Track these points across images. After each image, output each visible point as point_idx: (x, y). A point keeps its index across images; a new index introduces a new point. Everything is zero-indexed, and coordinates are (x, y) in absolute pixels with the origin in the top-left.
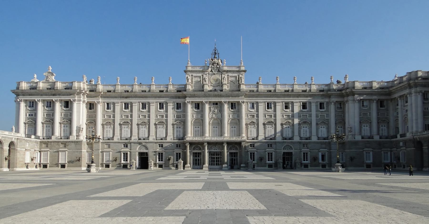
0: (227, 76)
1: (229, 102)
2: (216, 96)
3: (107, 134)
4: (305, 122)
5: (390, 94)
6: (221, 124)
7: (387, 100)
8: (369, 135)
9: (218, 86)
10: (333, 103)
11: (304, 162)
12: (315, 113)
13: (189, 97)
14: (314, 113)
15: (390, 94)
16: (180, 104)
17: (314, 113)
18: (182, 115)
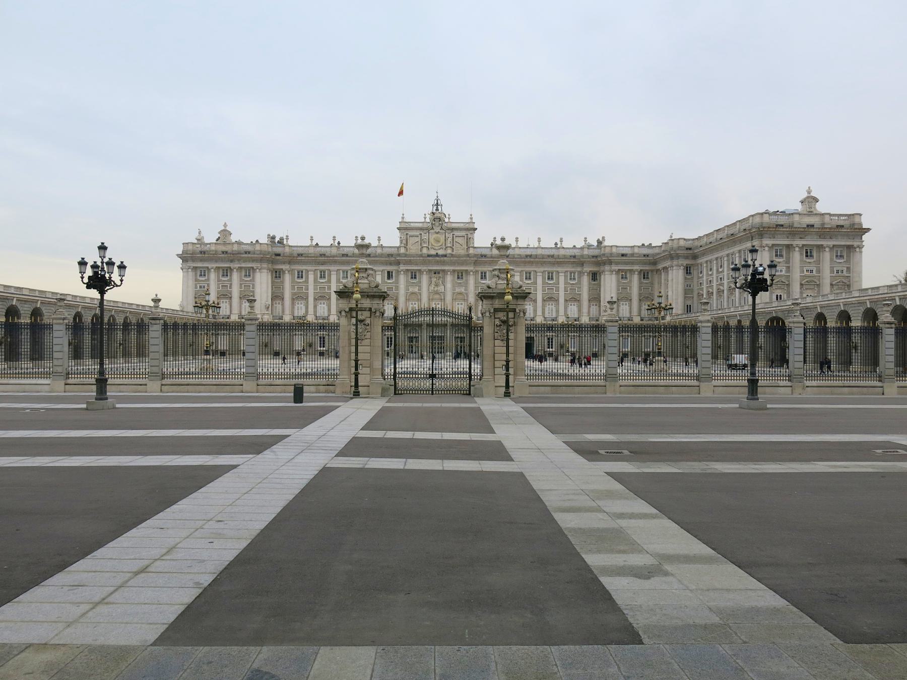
0: (451, 236)
1: (454, 271)
2: (438, 263)
3: (298, 312)
4: (550, 299)
5: (655, 263)
6: (444, 299)
7: (652, 271)
8: (628, 315)
9: (440, 249)
10: (586, 274)
11: (548, 350)
12: (563, 286)
13: (404, 264)
14: (562, 285)
15: (655, 263)
16: (392, 272)
17: (562, 285)
18: (394, 287)
